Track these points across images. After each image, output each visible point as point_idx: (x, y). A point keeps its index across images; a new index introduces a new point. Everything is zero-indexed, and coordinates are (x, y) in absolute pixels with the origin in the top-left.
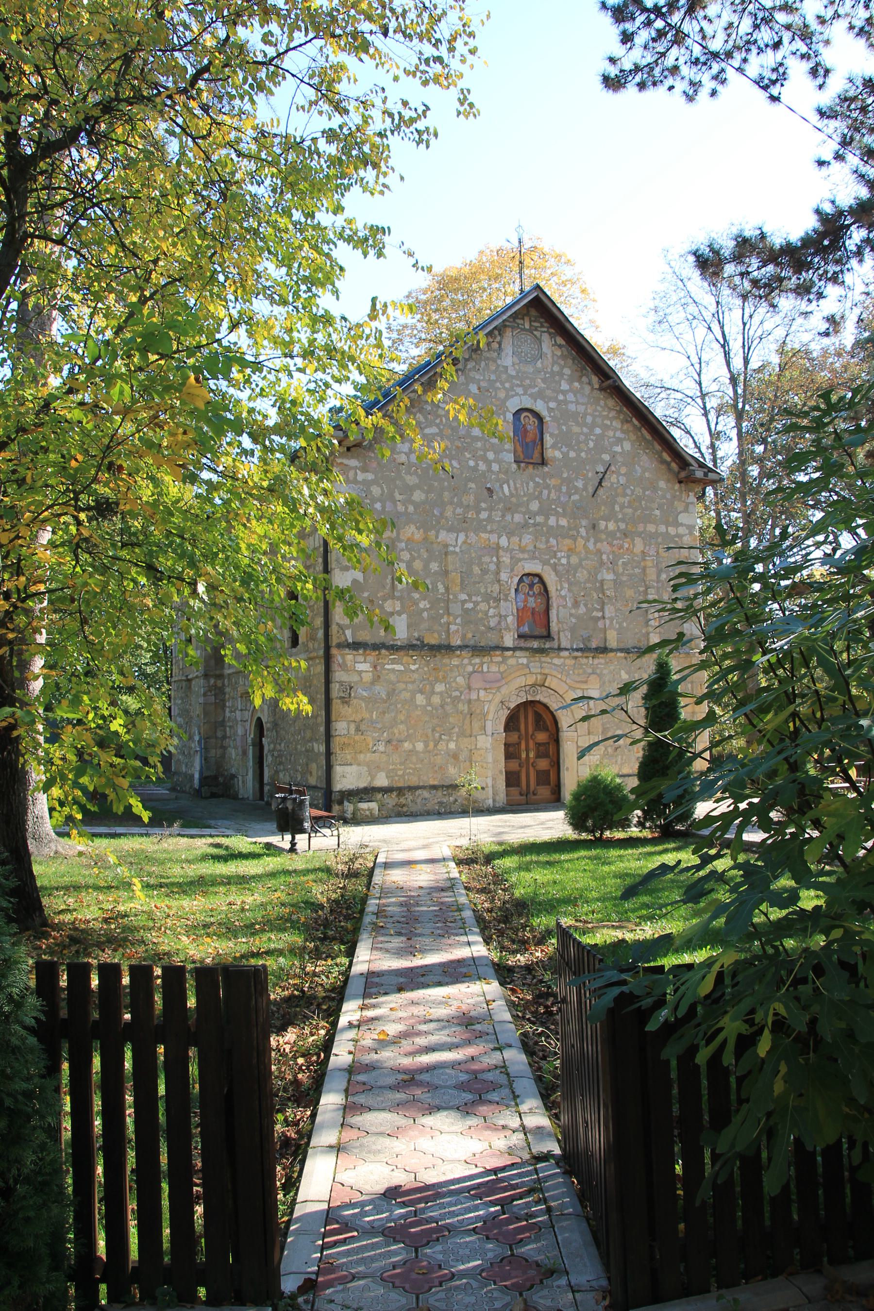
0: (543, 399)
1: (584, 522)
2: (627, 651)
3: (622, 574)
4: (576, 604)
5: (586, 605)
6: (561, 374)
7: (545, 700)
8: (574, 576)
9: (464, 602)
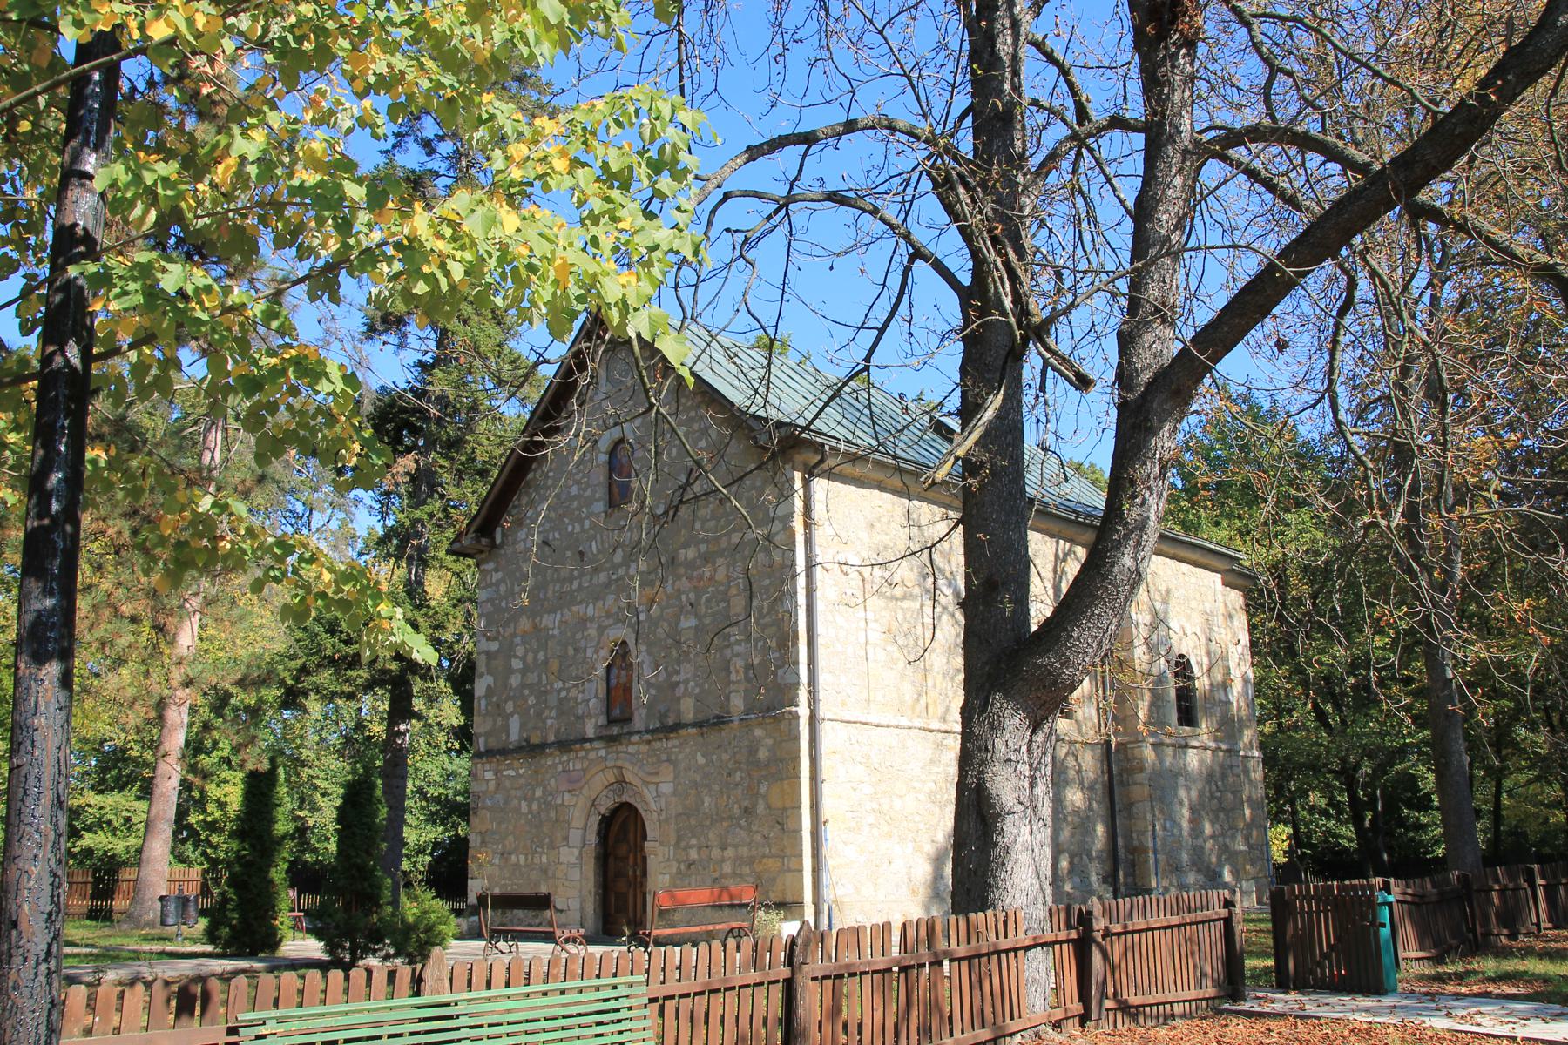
2: (699, 725)
9: (559, 691)
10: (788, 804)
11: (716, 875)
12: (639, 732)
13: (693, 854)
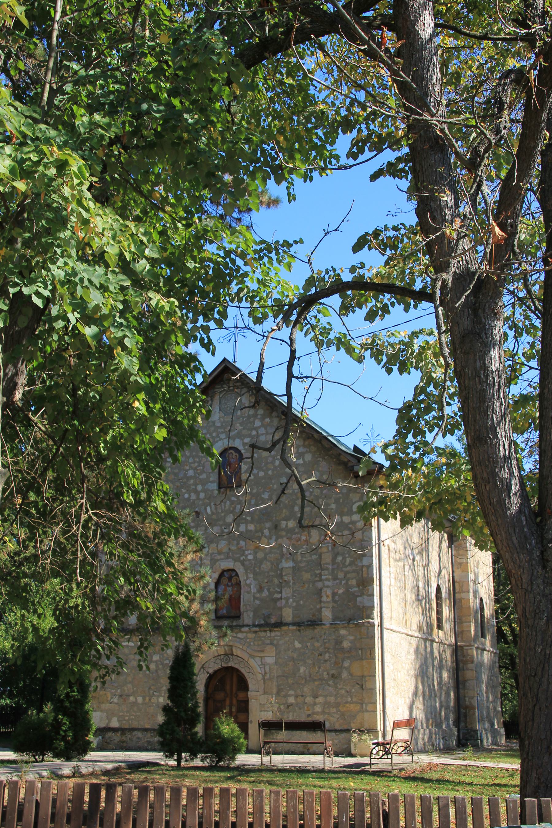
0: (239, 438)
1: (268, 525)
2: (299, 624)
3: (301, 561)
4: (261, 589)
5: (268, 590)
6: (255, 416)
7: (236, 666)
8: (260, 568)
10: (366, 673)
11: (310, 712)
12: (247, 626)
13: (291, 700)
